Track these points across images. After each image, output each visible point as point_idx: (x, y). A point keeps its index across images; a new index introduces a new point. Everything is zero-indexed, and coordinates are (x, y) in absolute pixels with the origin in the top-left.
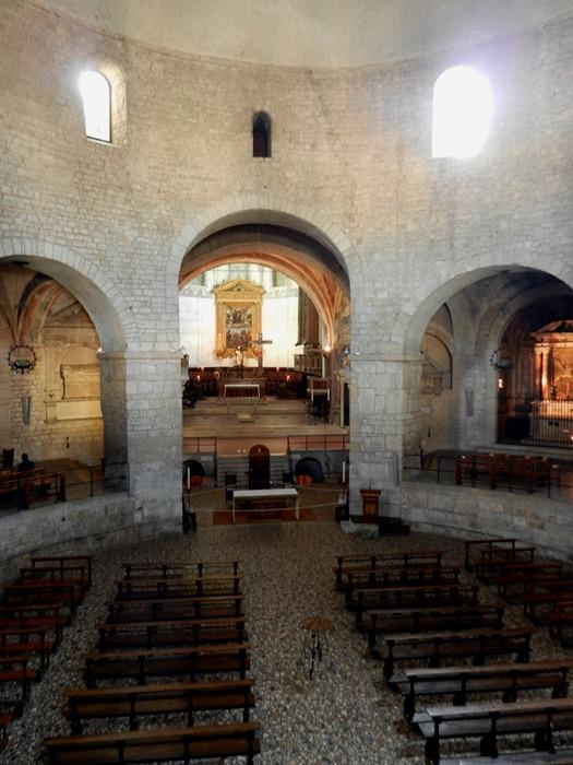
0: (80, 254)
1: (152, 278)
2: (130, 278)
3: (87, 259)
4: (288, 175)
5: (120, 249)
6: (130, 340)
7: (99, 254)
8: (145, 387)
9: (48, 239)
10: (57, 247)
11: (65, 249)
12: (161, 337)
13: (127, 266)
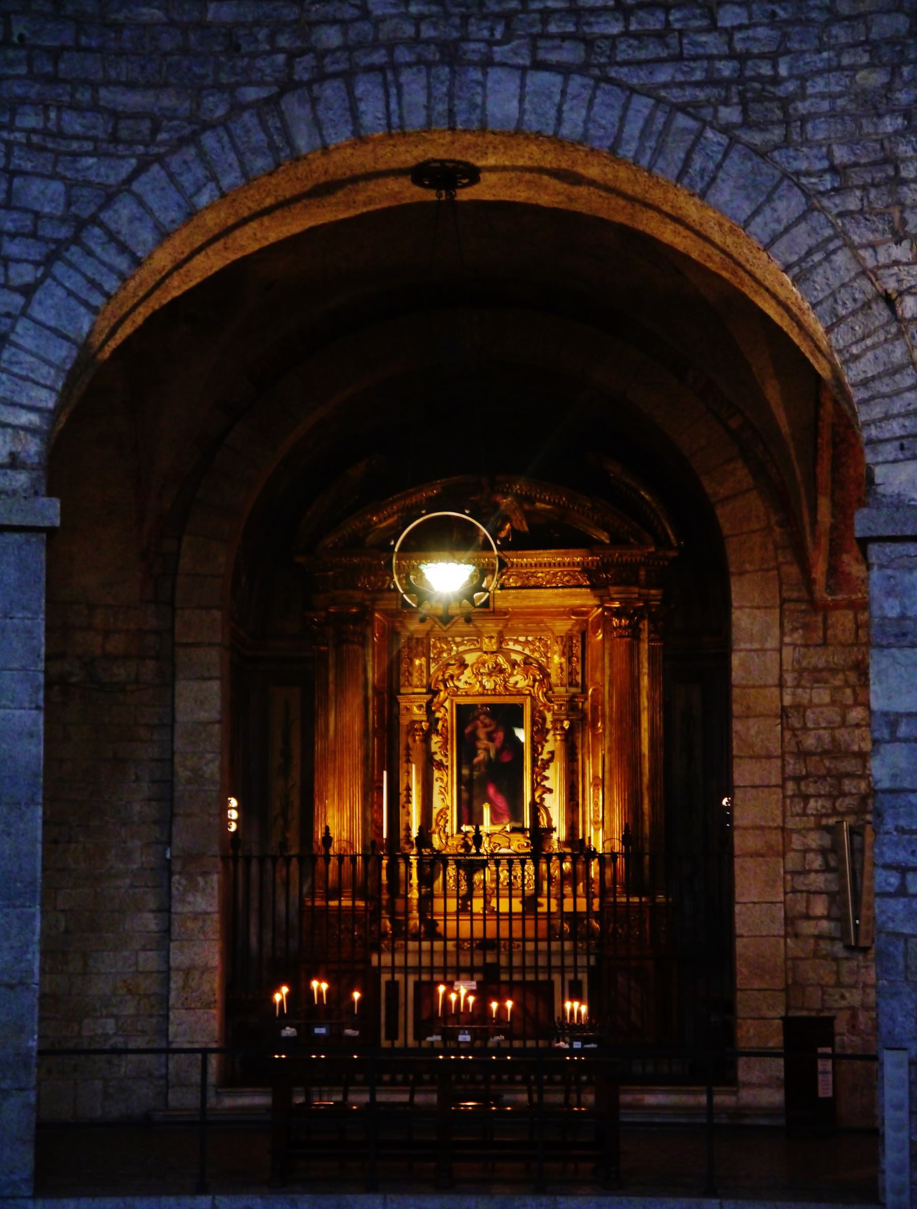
0: (647, 91)
2: (892, 160)
3: (682, 108)
5: (840, 34)
6: (889, 451)
7: (740, 79)
9: (499, 52)
10: (539, 79)
11: (576, 82)
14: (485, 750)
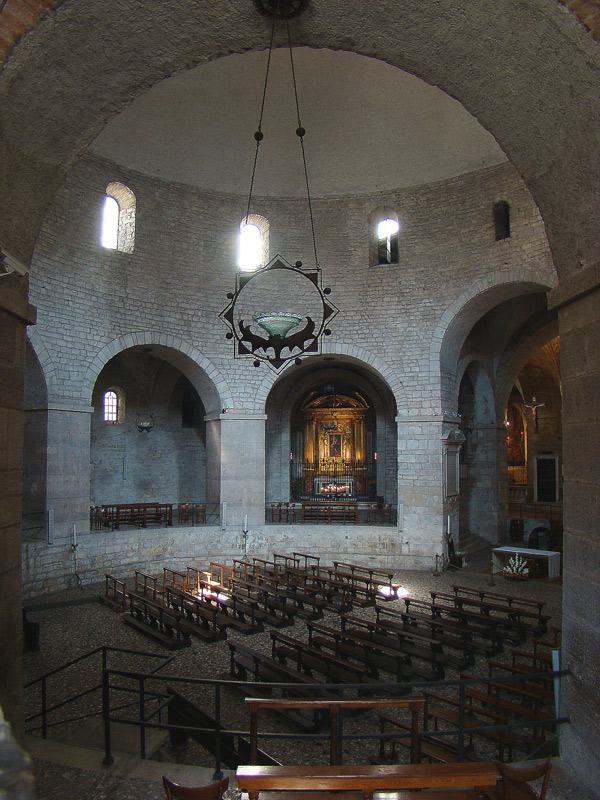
1: (417, 357)
4: (524, 247)
8: (412, 444)
12: (426, 404)
13: (399, 351)
14: (335, 442)
